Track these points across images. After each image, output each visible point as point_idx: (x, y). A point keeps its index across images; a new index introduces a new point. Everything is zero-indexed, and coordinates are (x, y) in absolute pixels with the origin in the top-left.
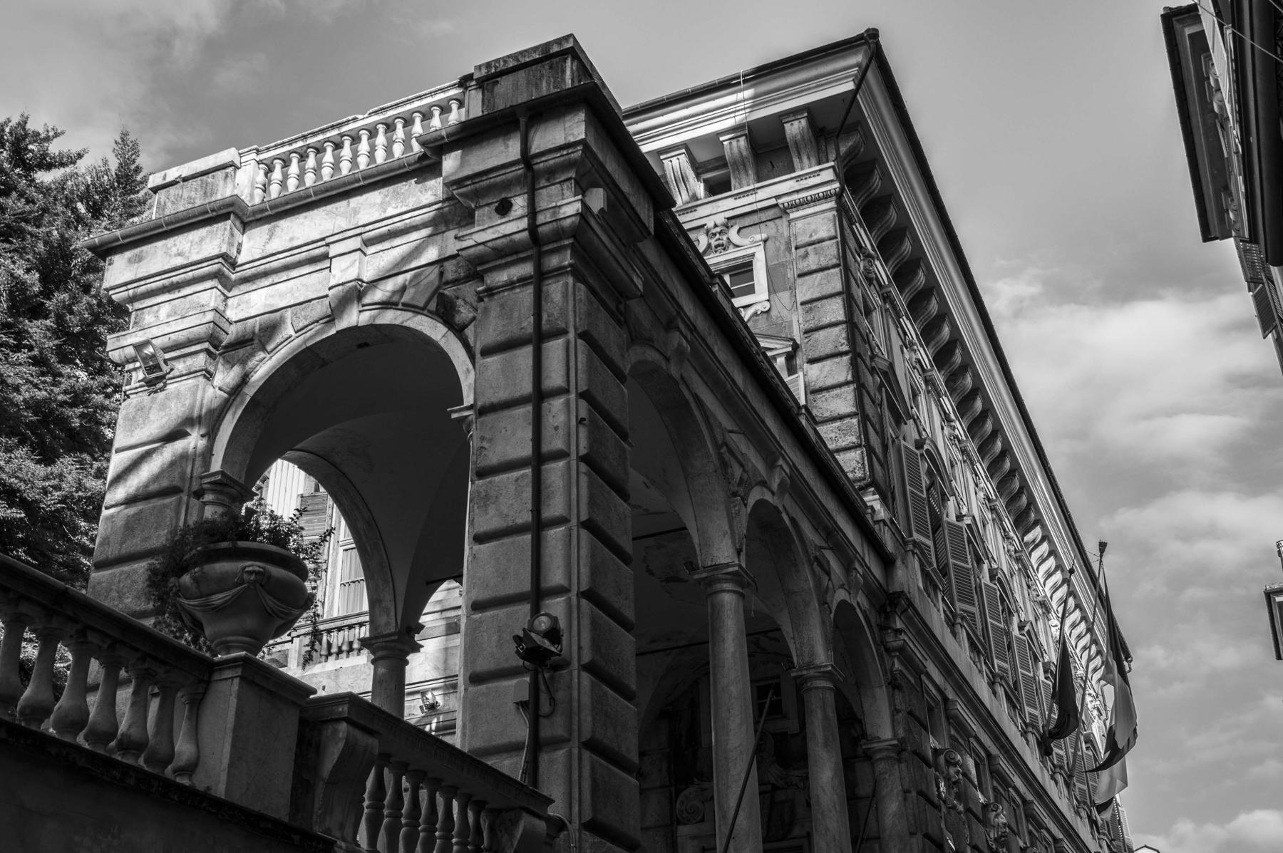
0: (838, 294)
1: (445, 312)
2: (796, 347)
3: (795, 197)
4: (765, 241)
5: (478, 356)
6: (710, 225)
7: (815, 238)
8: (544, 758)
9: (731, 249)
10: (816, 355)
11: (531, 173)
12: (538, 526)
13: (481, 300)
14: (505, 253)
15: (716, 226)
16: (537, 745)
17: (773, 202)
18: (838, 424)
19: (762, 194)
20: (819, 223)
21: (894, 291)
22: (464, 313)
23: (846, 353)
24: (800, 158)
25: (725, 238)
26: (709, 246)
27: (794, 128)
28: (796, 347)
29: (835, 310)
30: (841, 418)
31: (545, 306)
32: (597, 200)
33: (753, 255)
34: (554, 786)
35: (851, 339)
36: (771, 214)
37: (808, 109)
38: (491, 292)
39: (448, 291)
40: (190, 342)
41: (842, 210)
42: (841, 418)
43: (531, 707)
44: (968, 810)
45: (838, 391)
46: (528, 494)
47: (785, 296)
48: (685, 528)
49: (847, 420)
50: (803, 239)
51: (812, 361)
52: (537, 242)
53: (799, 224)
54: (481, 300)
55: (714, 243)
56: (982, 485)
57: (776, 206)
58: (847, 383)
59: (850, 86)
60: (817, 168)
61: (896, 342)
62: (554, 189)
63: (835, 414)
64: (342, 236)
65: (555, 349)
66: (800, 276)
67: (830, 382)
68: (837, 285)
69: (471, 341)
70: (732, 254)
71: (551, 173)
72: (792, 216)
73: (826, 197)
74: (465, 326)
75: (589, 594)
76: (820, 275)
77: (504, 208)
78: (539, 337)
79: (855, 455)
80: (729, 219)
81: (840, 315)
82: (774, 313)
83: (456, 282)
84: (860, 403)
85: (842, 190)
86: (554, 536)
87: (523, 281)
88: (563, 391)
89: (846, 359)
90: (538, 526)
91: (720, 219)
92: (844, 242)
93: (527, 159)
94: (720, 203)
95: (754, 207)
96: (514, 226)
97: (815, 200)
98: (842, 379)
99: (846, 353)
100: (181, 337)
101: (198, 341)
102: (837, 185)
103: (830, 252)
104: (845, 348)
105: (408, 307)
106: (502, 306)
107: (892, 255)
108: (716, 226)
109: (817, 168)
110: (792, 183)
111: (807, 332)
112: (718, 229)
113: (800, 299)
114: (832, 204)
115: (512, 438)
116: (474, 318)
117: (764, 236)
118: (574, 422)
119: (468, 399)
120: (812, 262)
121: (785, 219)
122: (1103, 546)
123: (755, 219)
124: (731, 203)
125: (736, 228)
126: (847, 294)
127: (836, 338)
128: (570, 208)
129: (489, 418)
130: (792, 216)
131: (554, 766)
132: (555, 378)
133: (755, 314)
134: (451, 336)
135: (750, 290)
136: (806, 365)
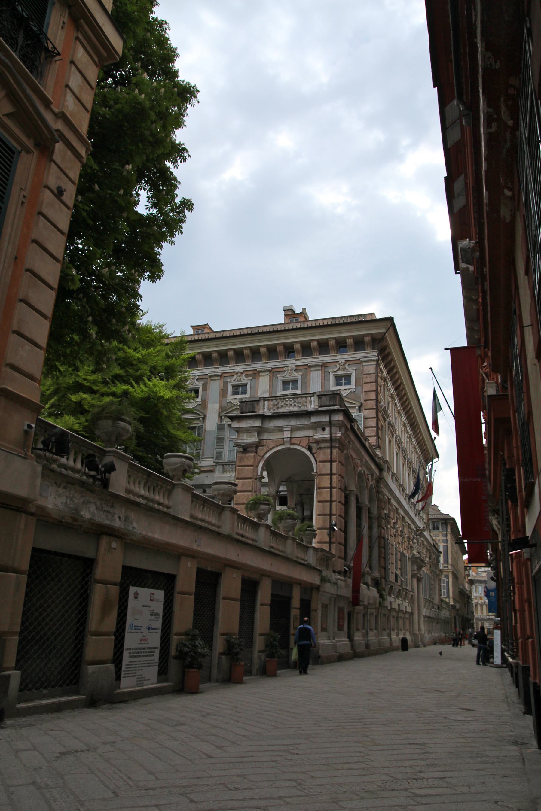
1: (310, 449)
2: (362, 404)
6: (340, 362)
8: (332, 545)
10: (367, 408)
11: (330, 424)
12: (331, 501)
14: (324, 441)
16: (330, 543)
17: (358, 358)
19: (356, 355)
20: (370, 368)
22: (314, 451)
29: (373, 396)
30: (372, 427)
31: (333, 455)
32: (343, 430)
34: (333, 552)
35: (377, 405)
36: (357, 362)
37: (371, 334)
38: (320, 448)
39: (310, 444)
41: (378, 365)
42: (372, 427)
43: (329, 535)
44: (391, 526)
46: (329, 494)
47: (359, 388)
52: (331, 440)
53: (366, 367)
56: (403, 420)
58: (374, 418)
59: (384, 331)
61: (386, 390)
62: (335, 428)
64: (287, 426)
65: (334, 464)
66: (365, 383)
70: (346, 372)
71: (334, 425)
72: (364, 364)
75: (340, 516)
77: (324, 429)
78: (331, 461)
79: (375, 438)
81: (375, 398)
82: (356, 392)
84: (377, 424)
86: (334, 504)
87: (328, 447)
88: (336, 474)
90: (331, 501)
91: (343, 361)
93: (330, 421)
95: (354, 359)
96: (326, 435)
103: (373, 379)
104: (375, 407)
105: (301, 446)
106: (323, 452)
111: (366, 400)
113: (364, 390)
115: (326, 482)
117: (355, 368)
119: (315, 471)
124: (346, 356)
127: (372, 404)
128: (339, 435)
129: (321, 477)
131: (334, 546)
132: (334, 471)
135: (349, 384)
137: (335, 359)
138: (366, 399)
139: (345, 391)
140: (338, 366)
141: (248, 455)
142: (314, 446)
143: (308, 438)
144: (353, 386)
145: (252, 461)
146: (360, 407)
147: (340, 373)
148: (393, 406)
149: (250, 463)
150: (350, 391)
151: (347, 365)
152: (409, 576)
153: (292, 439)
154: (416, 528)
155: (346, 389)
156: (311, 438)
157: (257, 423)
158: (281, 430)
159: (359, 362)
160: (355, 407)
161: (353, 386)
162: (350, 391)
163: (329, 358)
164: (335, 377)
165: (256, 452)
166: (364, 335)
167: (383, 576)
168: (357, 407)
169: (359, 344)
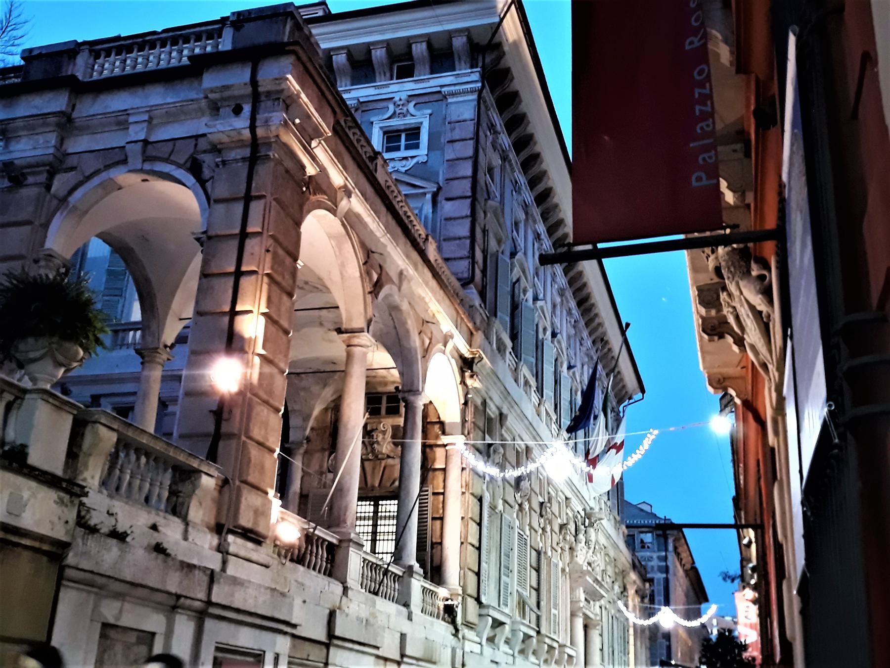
0: (470, 157)
3: (452, 88)
4: (430, 115)
5: (212, 202)
6: (397, 99)
7: (461, 118)
9: (409, 117)
10: (450, 196)
13: (217, 166)
15: (400, 100)
17: (438, 89)
18: (457, 242)
19: (433, 83)
21: (512, 155)
22: (206, 173)
23: (469, 197)
24: (460, 62)
25: (405, 109)
26: (395, 112)
27: (459, 42)
28: (439, 189)
29: (466, 169)
30: (460, 238)
33: (422, 123)
36: (437, 97)
37: (468, 30)
39: (201, 157)
40: (38, 165)
45: (461, 221)
48: (338, 307)
49: (463, 240)
50: (454, 118)
51: (448, 199)
54: (217, 166)
55: (398, 111)
57: (440, 92)
58: (467, 217)
60: (470, 71)
61: (509, 186)
63: (457, 235)
67: (457, 215)
68: (470, 152)
69: (209, 190)
70: (410, 121)
73: (472, 91)
74: (207, 181)
76: (461, 143)
77: (238, 110)
80: (410, 96)
81: (469, 172)
82: (429, 163)
83: (205, 152)
85: (483, 86)
87: (243, 159)
89: (469, 200)
91: (404, 96)
92: (478, 124)
94: (405, 84)
97: (465, 92)
98: (464, 214)
99: (469, 197)
100: (32, 161)
101: (44, 165)
102: (479, 85)
107: (514, 130)
108: (400, 100)
109: (470, 71)
110: (452, 78)
112: (401, 103)
113: (447, 157)
114: (475, 96)
116: (212, 177)
117: (429, 111)
118: (263, 251)
120: (457, 135)
121: (444, 103)
122: (628, 325)
123: (426, 99)
124: (412, 86)
125: (413, 103)
126: (475, 159)
127: (465, 187)
130: (449, 100)
133: (417, 163)
134: (198, 185)
135: (417, 146)
136: (444, 202)
137: (385, 93)
138: (451, 176)
139: (404, 162)
140: (392, 108)
141: (24, 192)
142: (208, 159)
143: (193, 142)
144: (422, 152)
145: (31, 209)
146: (435, 196)
147: (396, 123)
148: (565, 312)
149: (21, 217)
150: (415, 160)
151: (412, 104)
152: (562, 612)
153: (150, 147)
154: (584, 510)
155: (405, 158)
156: (201, 141)
157: (55, 102)
158: (121, 121)
159: (439, 97)
160: (425, 194)
161: (422, 152)
162: (415, 160)
163: (372, 91)
164: (385, 133)
165: (48, 187)
166: (450, 34)
167: (472, 590)
168: (429, 196)
169: (441, 56)
